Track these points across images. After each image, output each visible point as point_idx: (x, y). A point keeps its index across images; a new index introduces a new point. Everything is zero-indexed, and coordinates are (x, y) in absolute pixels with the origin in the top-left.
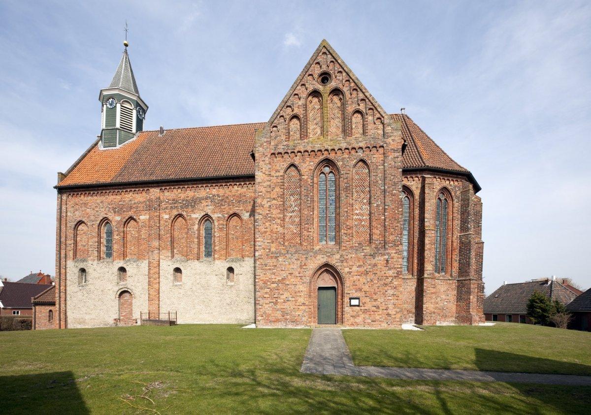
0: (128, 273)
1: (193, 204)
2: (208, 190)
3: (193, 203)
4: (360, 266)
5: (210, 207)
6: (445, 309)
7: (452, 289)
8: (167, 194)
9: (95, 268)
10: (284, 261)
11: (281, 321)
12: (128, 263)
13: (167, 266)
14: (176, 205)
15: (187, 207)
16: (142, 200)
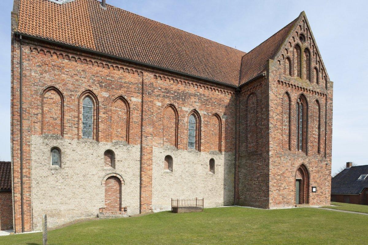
0: (117, 158)
1: (183, 98)
2: (196, 88)
3: (184, 97)
5: (198, 104)
8: (159, 81)
9: (71, 147)
10: (284, 160)
11: (281, 203)
12: (117, 146)
13: (158, 153)
14: (168, 95)
15: (178, 99)
16: (133, 80)
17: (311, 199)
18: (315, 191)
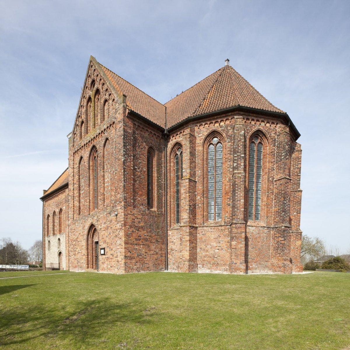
4: (105, 223)
6: (216, 256)
7: (225, 236)
17: (100, 263)
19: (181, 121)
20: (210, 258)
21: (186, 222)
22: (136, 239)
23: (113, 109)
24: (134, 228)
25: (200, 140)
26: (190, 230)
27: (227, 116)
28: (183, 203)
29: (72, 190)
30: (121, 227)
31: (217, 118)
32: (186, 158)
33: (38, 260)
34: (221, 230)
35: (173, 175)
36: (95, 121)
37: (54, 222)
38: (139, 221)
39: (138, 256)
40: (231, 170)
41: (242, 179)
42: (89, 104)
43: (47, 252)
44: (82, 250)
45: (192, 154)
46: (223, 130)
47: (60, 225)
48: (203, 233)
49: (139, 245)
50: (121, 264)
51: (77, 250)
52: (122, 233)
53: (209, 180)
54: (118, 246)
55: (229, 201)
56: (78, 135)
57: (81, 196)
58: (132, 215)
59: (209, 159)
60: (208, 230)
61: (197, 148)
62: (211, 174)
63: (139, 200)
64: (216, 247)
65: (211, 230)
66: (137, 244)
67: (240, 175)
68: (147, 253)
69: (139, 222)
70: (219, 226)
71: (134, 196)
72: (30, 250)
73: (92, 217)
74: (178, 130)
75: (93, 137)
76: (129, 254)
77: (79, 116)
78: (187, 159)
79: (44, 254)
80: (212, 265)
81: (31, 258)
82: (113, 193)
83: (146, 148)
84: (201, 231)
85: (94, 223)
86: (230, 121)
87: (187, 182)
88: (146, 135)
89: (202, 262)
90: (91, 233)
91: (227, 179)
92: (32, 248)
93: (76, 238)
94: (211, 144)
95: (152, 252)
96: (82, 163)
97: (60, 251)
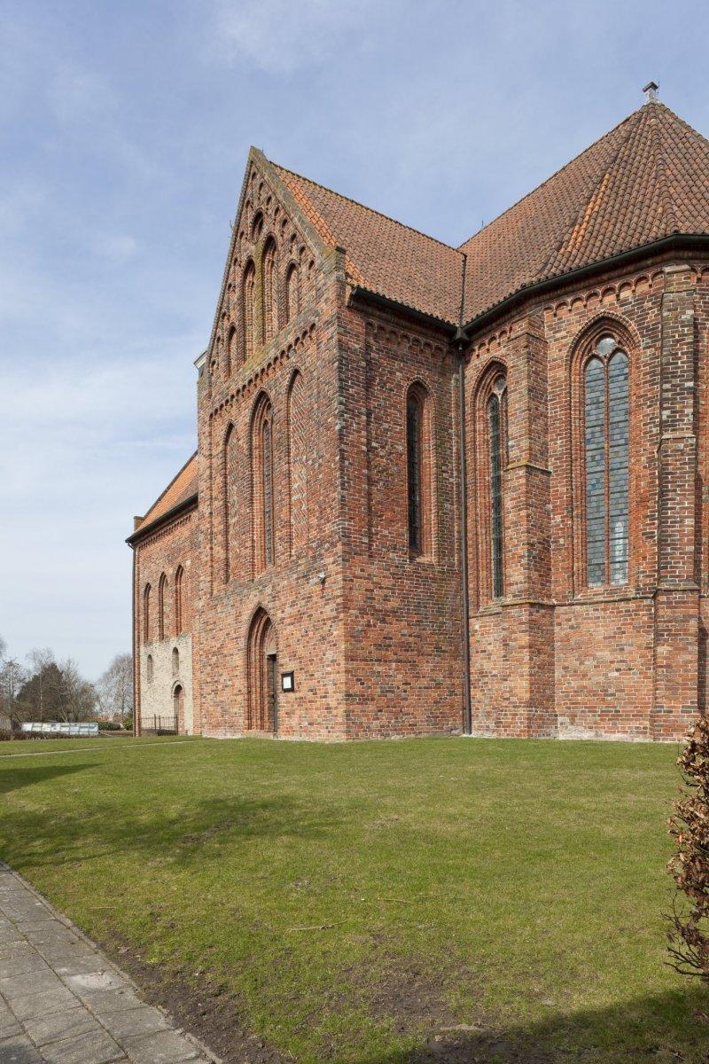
6: (611, 691)
7: (637, 629)
17: (281, 713)
18: (290, 687)
19: (502, 299)
20: (594, 695)
21: (519, 592)
22: (378, 647)
23: (311, 288)
24: (372, 615)
25: (560, 350)
26: (531, 614)
27: (642, 269)
28: (511, 539)
29: (207, 515)
30: (334, 613)
31: (610, 279)
32: (517, 406)
33: (121, 710)
34: (626, 611)
35: (482, 457)
36: (264, 325)
37: (161, 604)
38: (386, 596)
39: (384, 693)
40: (654, 433)
41: (689, 455)
42: (249, 278)
43: (144, 686)
44: (235, 680)
45: (536, 393)
46: (630, 314)
47: (178, 612)
48: (573, 622)
49: (385, 661)
50: (336, 716)
51: (222, 681)
52: (338, 631)
53: (588, 465)
54: (328, 666)
55: (650, 524)
56: (222, 364)
57: (232, 531)
58: (365, 578)
59: (588, 402)
60: (588, 614)
61: (550, 374)
62: (594, 446)
63: (385, 536)
64: (612, 662)
65: (597, 614)
66: (380, 660)
67: (681, 446)
68: (410, 684)
69: (386, 599)
70: (619, 601)
71: (370, 525)
72: (100, 681)
73: (261, 588)
74: (494, 325)
75: (258, 369)
76: (357, 688)
77: (224, 314)
78: (519, 409)
79: (137, 693)
80: (599, 716)
81: (102, 706)
82: (314, 521)
83: (402, 387)
84: (567, 617)
85: (265, 604)
86: (650, 282)
87: (520, 477)
88: (404, 349)
89: (569, 708)
90: (258, 631)
91: (643, 458)
92: (107, 677)
93: (219, 645)
94: (594, 356)
95: (425, 682)
96: (233, 440)
97: (178, 683)
